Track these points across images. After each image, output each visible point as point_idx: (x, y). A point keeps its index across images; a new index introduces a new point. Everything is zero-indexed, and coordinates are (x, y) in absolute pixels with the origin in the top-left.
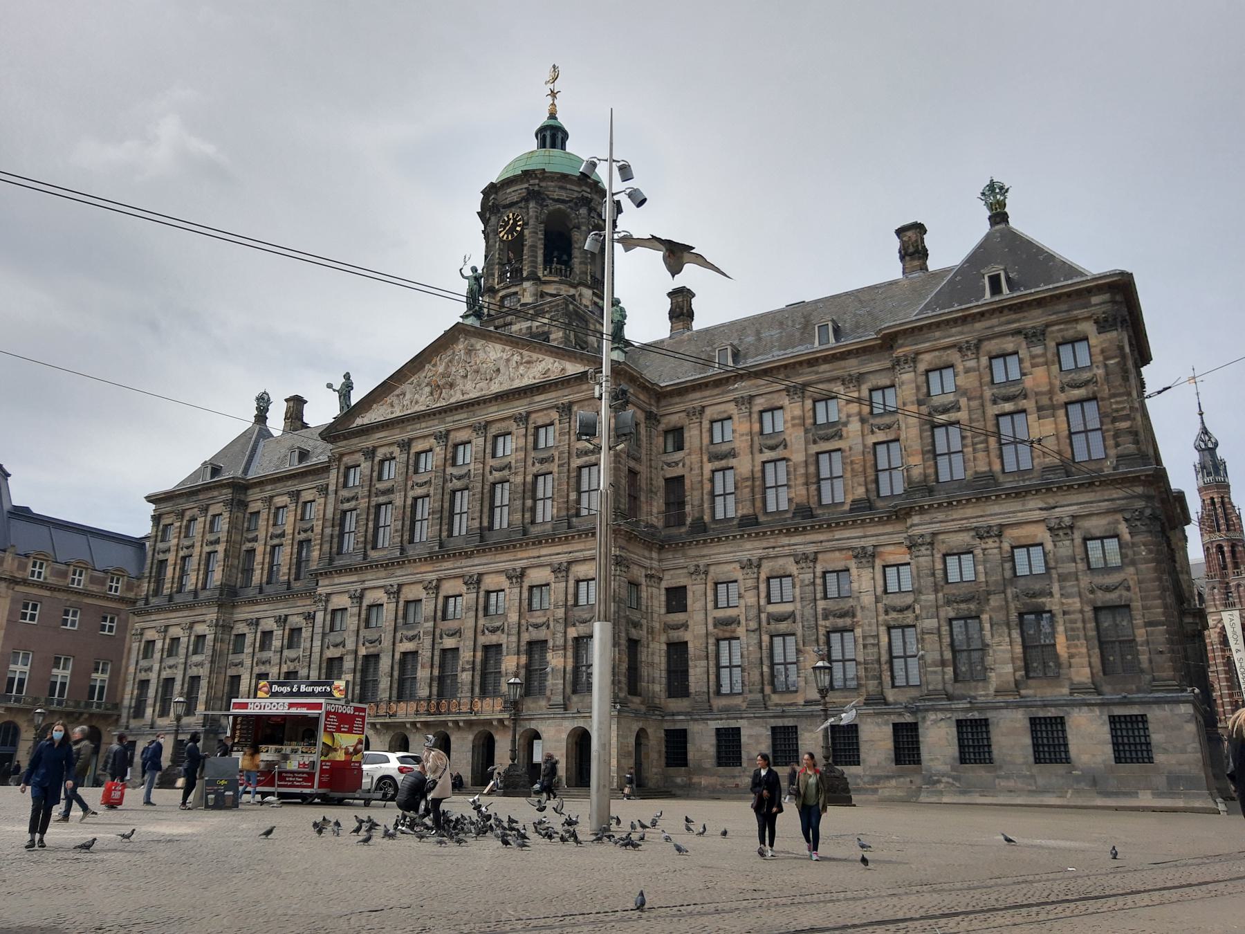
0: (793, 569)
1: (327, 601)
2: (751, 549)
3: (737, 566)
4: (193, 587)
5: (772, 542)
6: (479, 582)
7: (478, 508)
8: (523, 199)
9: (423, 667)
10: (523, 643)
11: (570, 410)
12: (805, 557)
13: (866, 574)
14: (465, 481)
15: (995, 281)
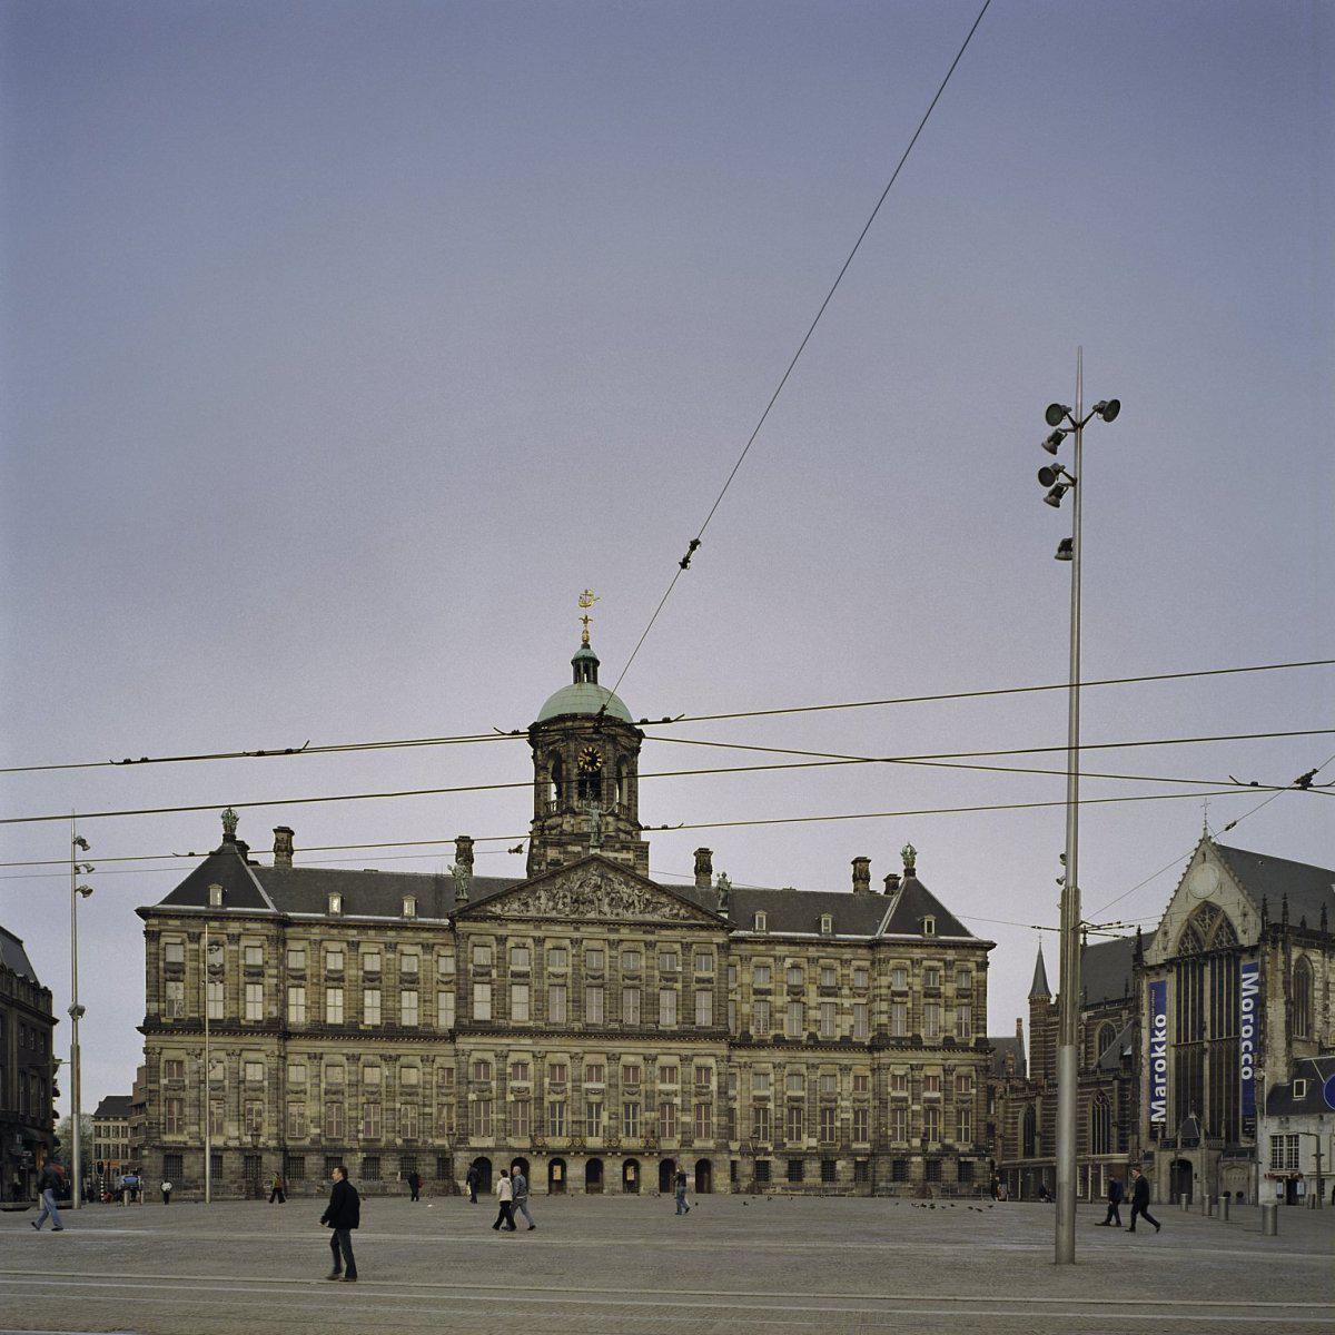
0: (804, 1071)
1: (469, 1056)
2: (780, 1056)
3: (770, 1065)
4: (233, 1016)
5: (793, 1054)
9: (573, 1113)
10: (656, 1104)
12: (813, 1065)
13: (845, 1079)
14: (599, 981)
15: (929, 924)
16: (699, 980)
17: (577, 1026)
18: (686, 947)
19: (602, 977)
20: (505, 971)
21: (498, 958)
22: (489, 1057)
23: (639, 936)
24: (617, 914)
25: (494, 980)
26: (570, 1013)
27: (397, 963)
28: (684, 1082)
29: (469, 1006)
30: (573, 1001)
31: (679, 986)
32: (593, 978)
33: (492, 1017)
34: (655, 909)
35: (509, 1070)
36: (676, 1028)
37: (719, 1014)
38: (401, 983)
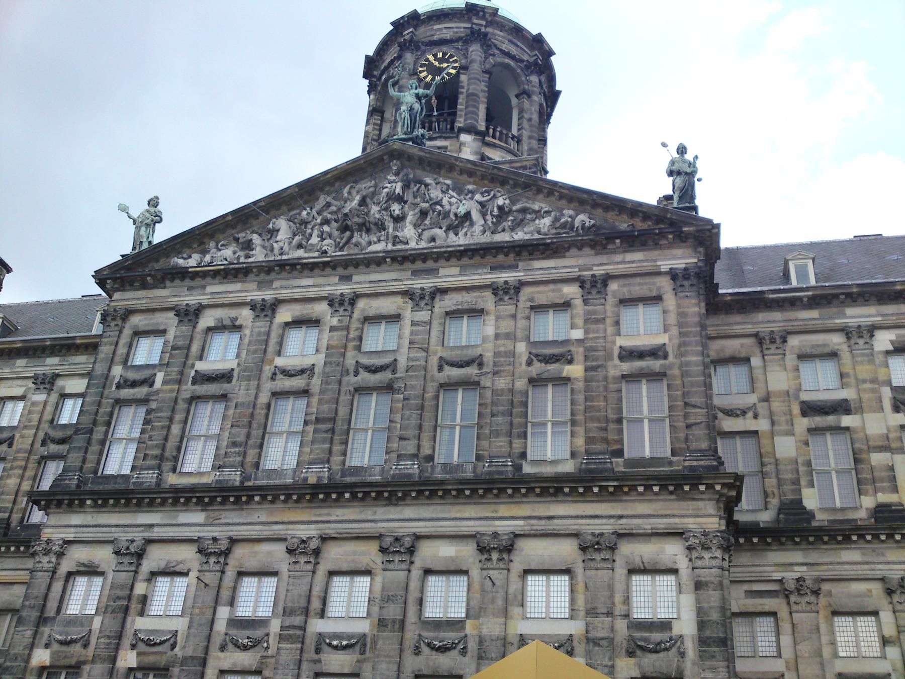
1: (60, 555)
6: (411, 551)
7: (414, 422)
8: (458, 40)
11: (606, 285)
14: (386, 376)
16: (628, 354)
17: (315, 474)
18: (594, 286)
19: (392, 366)
20: (182, 373)
21: (174, 348)
22: (103, 556)
23: (485, 277)
24: (433, 239)
25: (157, 392)
26: (307, 449)
27: (49, 409)
28: (591, 612)
29: (95, 448)
30: (318, 420)
31: (575, 370)
32: (374, 370)
33: (133, 468)
34: (518, 225)
35: (140, 588)
36: (569, 467)
37: (688, 426)
38: (44, 443)
